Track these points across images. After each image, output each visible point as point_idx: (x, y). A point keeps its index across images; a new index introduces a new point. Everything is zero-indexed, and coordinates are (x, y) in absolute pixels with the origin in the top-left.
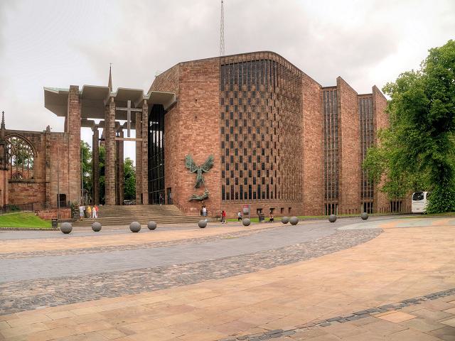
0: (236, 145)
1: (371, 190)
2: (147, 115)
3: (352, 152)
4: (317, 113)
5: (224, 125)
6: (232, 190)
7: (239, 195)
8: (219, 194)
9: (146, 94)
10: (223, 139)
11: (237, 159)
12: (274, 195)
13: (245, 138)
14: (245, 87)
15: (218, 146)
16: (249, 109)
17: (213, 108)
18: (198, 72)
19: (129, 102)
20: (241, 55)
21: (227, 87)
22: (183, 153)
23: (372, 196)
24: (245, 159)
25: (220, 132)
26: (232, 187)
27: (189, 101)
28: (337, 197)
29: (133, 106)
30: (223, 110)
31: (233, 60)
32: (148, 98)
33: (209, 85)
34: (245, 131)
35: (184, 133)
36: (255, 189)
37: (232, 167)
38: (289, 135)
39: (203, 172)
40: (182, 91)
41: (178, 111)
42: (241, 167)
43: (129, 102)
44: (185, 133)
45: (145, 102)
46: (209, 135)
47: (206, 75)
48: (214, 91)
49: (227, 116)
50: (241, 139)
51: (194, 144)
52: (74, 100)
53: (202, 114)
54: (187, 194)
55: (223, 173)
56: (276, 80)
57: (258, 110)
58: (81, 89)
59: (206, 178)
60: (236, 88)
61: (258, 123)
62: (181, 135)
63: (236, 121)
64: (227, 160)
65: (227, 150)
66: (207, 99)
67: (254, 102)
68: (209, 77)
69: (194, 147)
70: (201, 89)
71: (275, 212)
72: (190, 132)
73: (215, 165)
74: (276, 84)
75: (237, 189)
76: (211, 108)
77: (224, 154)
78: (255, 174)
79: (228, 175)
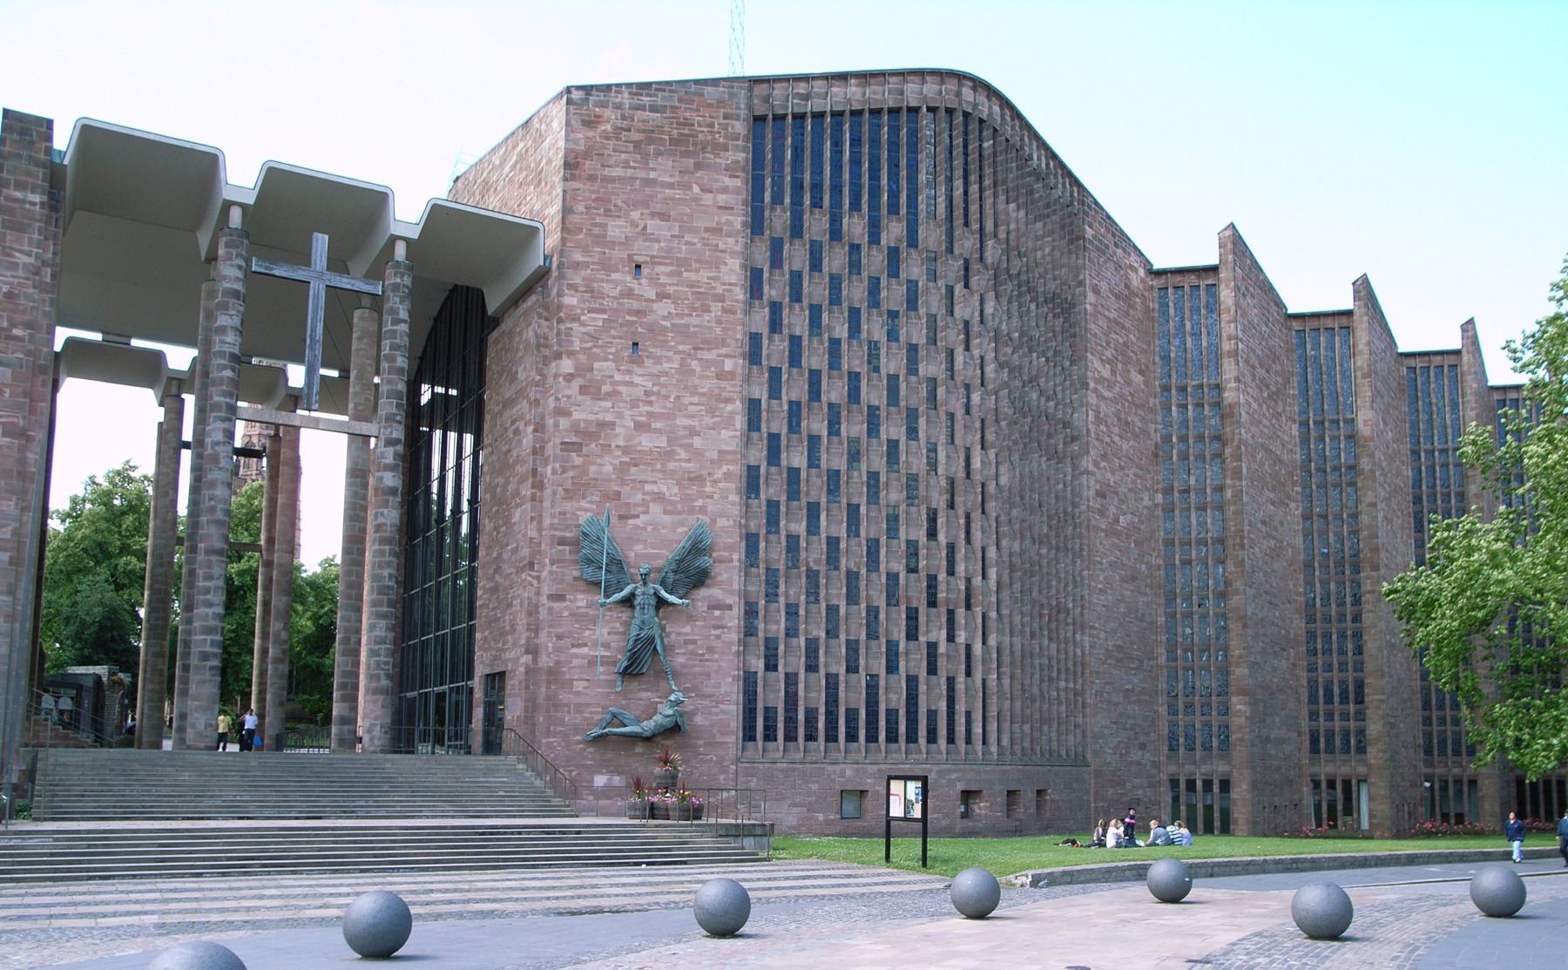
0: (815, 488)
1: (1352, 725)
2: (403, 315)
3: (1275, 554)
4: (1137, 378)
5: (760, 392)
6: (791, 699)
7: (821, 725)
8: (732, 711)
9: (407, 214)
10: (758, 455)
11: (814, 554)
12: (977, 729)
13: (854, 457)
14: (856, 227)
15: (732, 486)
16: (874, 328)
17: (716, 308)
18: (650, 135)
19: (321, 242)
21: (779, 220)
22: (568, 506)
24: (853, 556)
25: (740, 422)
26: (791, 679)
27: (607, 266)
29: (337, 263)
30: (760, 320)
31: (806, 97)
32: (414, 234)
33: (697, 199)
34: (853, 427)
35: (576, 416)
36: (893, 697)
37: (793, 590)
38: (1038, 463)
39: (661, 603)
41: (551, 311)
42: (836, 592)
43: (321, 242)
44: (585, 412)
45: (400, 251)
46: (693, 432)
47: (685, 154)
48: (716, 231)
50: (834, 459)
51: (622, 469)
52: (20, 186)
53: (664, 330)
54: (579, 708)
55: (750, 612)
56: (989, 203)
57: (915, 331)
58: (62, 140)
59: (678, 632)
60: (817, 225)
61: (913, 394)
62: (564, 423)
63: (815, 377)
64: (774, 552)
65: (773, 505)
66: (684, 263)
67: (894, 295)
68: (698, 166)
69: (623, 482)
70: (664, 217)
71: (980, 808)
72: (603, 411)
73: (724, 577)
74: (989, 226)
75: (812, 695)
77: (758, 524)
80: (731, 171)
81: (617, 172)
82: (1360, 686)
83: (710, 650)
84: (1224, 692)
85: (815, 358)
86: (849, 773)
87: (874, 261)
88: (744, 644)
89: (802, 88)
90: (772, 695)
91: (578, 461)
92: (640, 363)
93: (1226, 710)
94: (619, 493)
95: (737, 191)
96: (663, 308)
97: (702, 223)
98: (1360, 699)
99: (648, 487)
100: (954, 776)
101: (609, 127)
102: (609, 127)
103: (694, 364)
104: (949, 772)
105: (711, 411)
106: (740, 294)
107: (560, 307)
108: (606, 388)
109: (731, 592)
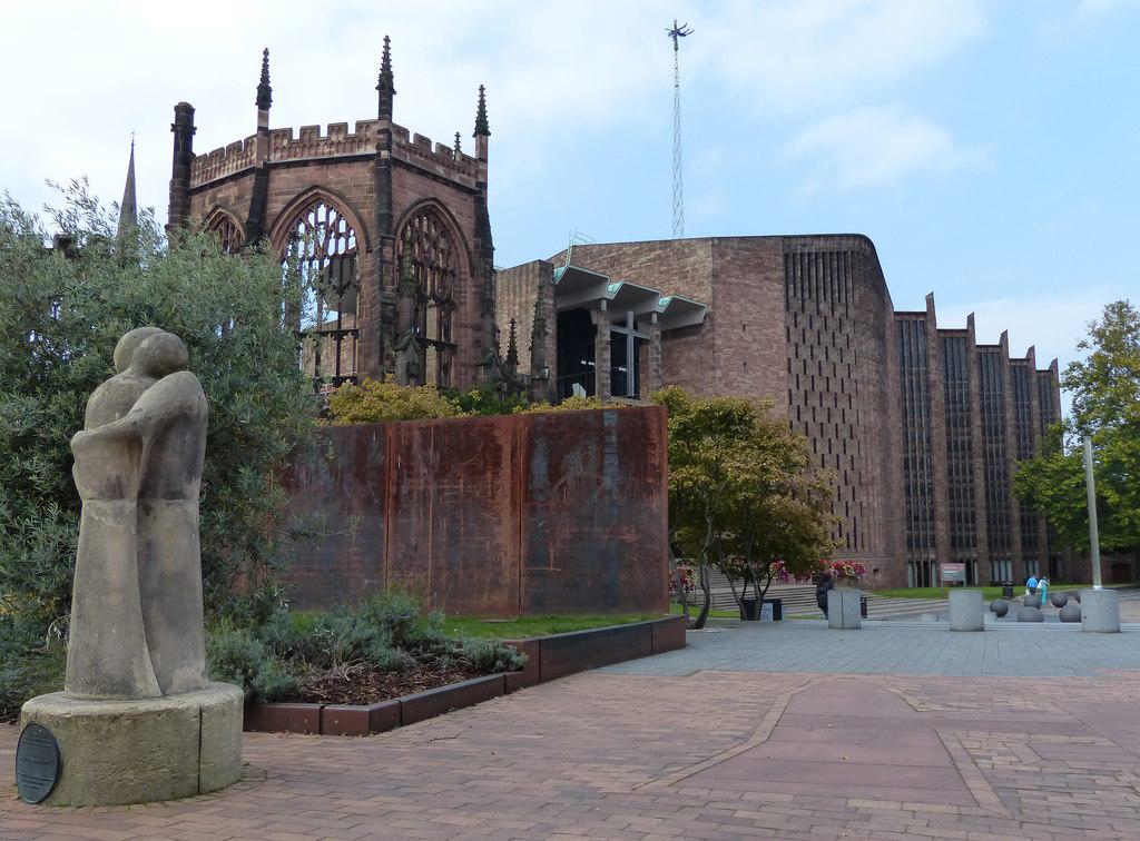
16: (834, 357)
19: (631, 316)
20: (819, 236)
21: (796, 305)
23: (975, 545)
25: (787, 400)
28: (933, 545)
31: (804, 246)
34: (829, 402)
40: (718, 303)
47: (761, 272)
49: (797, 366)
67: (840, 341)
68: (767, 279)
70: (754, 303)
71: (879, 577)
76: (772, 347)
80: (778, 281)
81: (734, 280)
82: (973, 514)
84: (932, 519)
85: (813, 370)
87: (833, 325)
89: (802, 241)
92: (747, 373)
93: (933, 529)
95: (780, 291)
96: (755, 346)
97: (769, 305)
98: (973, 522)
101: (729, 258)
102: (729, 258)
103: (769, 373)
105: (776, 396)
106: (784, 340)
107: (713, 346)
108: (735, 385)
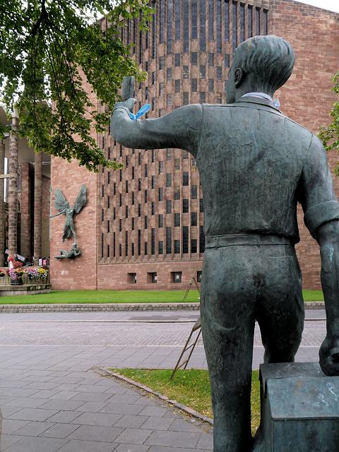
11: (120, 189)
37: (114, 203)
42: (127, 200)
51: (67, 171)
69: (67, 176)
73: (92, 202)
78: (146, 210)
79: (109, 216)
83: (89, 227)
86: (130, 267)
88: (99, 223)
90: (109, 241)
91: (56, 172)
94: (66, 180)
99: (73, 176)
100: (167, 266)
104: (165, 265)
109: (94, 207)
